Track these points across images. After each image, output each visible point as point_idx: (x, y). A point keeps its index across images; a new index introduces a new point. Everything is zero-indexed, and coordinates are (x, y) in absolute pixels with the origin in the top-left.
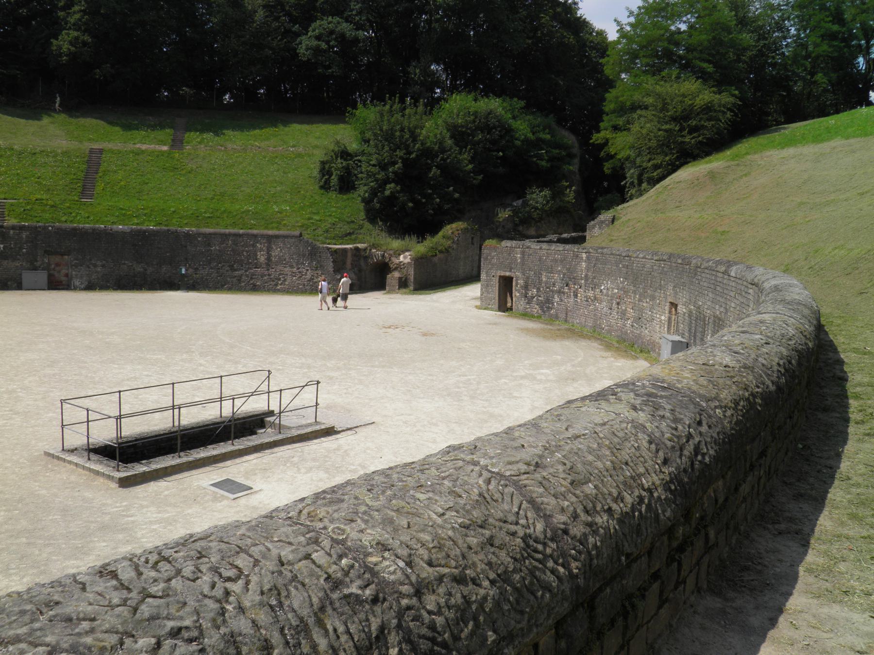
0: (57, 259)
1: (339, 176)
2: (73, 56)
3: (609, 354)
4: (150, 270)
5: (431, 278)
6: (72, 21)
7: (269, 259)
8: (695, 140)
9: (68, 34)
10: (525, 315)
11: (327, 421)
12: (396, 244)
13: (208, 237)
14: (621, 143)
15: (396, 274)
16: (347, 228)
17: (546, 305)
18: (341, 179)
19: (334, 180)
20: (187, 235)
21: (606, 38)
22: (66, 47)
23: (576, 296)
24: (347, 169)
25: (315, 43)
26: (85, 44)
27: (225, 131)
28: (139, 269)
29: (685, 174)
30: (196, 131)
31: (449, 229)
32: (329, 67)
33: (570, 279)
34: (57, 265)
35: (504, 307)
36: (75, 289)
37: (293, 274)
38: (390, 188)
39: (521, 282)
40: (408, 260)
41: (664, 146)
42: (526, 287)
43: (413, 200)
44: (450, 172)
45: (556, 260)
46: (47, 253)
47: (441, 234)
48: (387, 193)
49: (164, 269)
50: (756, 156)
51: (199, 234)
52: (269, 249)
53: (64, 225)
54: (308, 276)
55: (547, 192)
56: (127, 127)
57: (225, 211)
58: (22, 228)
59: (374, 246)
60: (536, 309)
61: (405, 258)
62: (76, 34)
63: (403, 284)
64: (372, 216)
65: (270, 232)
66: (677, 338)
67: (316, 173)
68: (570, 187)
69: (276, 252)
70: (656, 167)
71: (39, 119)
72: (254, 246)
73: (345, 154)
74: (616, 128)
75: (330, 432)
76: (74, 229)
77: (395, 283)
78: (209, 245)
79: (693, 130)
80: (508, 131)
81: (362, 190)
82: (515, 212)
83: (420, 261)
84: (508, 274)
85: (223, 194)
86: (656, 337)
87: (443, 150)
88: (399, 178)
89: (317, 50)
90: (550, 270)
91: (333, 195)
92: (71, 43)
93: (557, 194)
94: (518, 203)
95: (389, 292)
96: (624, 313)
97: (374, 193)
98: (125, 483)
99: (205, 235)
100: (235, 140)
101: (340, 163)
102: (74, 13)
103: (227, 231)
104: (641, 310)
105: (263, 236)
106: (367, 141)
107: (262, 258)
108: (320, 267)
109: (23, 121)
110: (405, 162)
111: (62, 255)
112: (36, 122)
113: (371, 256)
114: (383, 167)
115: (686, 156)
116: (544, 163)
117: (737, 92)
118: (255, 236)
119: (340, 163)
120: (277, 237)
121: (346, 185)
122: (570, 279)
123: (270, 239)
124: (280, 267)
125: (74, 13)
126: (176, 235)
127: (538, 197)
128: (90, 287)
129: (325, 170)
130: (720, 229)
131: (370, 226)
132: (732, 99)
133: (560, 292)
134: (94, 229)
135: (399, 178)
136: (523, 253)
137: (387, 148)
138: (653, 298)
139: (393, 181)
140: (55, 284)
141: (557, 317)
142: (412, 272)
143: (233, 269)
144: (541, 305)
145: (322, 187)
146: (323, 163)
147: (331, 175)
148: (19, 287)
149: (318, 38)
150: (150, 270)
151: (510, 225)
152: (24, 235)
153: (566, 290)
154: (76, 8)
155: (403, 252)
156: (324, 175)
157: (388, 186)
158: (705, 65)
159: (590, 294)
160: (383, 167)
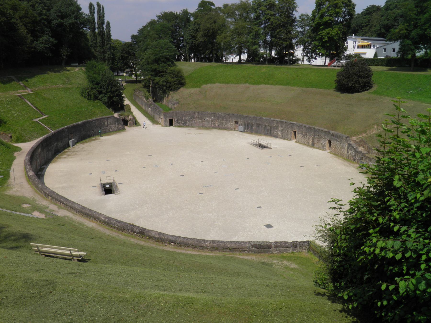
23: (195, 121)
33: (193, 118)
42: (178, 120)
52: (107, 121)
60: (181, 125)
105: (106, 118)
107: (106, 124)
120: (109, 117)
121: (96, 98)
123: (108, 118)
133: (189, 121)
136: (176, 113)
139: (115, 97)
144: (183, 124)
145: (88, 99)
156: (89, 95)
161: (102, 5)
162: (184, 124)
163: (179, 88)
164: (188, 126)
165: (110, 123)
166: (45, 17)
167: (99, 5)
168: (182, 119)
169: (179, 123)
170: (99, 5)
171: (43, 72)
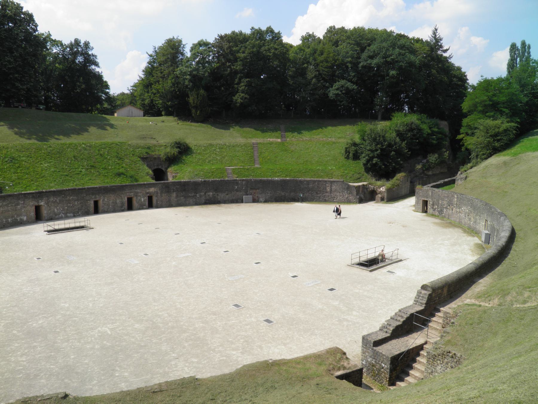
0: (254, 191)
1: (353, 153)
2: (241, 104)
3: (465, 235)
4: (287, 194)
5: (393, 197)
6: (241, 89)
7: (331, 190)
8: (500, 144)
9: (240, 95)
10: (433, 215)
11: (400, 258)
12: (379, 183)
13: (308, 182)
14: (470, 142)
15: (380, 196)
16: (358, 176)
17: (441, 212)
18: (354, 154)
19: (351, 155)
20: (301, 181)
21: (462, 78)
22: (239, 100)
23: (452, 210)
24: (356, 151)
25: (337, 92)
26: (246, 98)
27: (302, 132)
28: (283, 194)
29: (495, 160)
30: (290, 132)
31: (400, 176)
32: (342, 101)
33: (450, 204)
34: (254, 193)
35: (425, 211)
36: (261, 202)
37: (340, 196)
38: (375, 160)
39: (431, 203)
40: (384, 190)
41: (487, 146)
42: (433, 205)
43: (384, 164)
44: (399, 152)
45: (445, 196)
46: (251, 189)
47: (395, 178)
48: (374, 162)
49: (292, 194)
50: (523, 155)
51: (305, 181)
52: (331, 186)
53: (257, 179)
54: (346, 197)
55: (436, 155)
56: (263, 131)
57: (310, 170)
58: (243, 180)
59: (370, 184)
60: (437, 213)
61: (383, 189)
62: (243, 95)
63: (382, 199)
64: (367, 170)
65: (332, 180)
66: (487, 232)
67: (343, 151)
68: (446, 152)
69: (334, 187)
70: (484, 154)
71: (229, 130)
72: (325, 185)
73: (355, 144)
74: (467, 134)
75: (401, 261)
76: (261, 180)
77: (380, 199)
78: (309, 185)
79: (498, 141)
80: (420, 130)
81: (363, 160)
82: (424, 166)
83: (389, 190)
84: (426, 199)
85: (307, 161)
86: (481, 229)
87: (395, 144)
88: (378, 156)
89: (337, 95)
90: (443, 200)
91: (351, 161)
92: (241, 99)
93: (441, 155)
94: (425, 161)
95: (377, 202)
96: (470, 219)
97: (368, 161)
98: (371, 271)
99: (307, 181)
100: (306, 136)
101: (353, 148)
102: (242, 86)
103: (315, 179)
104: (476, 219)
105: (329, 181)
106: (364, 140)
107: (328, 189)
108: (351, 193)
109: (223, 131)
110: (382, 150)
111: (256, 189)
112: (228, 131)
113: (369, 188)
114: (372, 151)
115: (495, 151)
116: (435, 142)
117: (519, 120)
118: (326, 181)
119: (353, 148)
120: (334, 182)
121: (356, 157)
122: (450, 204)
123: (332, 182)
124: (335, 193)
125: (242, 86)
126: (296, 181)
127: (433, 158)
128: (266, 201)
129: (347, 151)
130: (505, 190)
131: (367, 175)
132: (516, 125)
133: (446, 208)
134: (267, 180)
135: (378, 156)
136: (432, 192)
137: (374, 144)
138: (480, 216)
139: (376, 157)
140: (255, 201)
141: (445, 217)
142: (386, 194)
143: (317, 193)
144: (439, 212)
145: (345, 158)
146: (346, 148)
147: (350, 153)
148: (242, 202)
149: (337, 89)
150: (287, 194)
151: (421, 171)
152: (244, 183)
153: (449, 207)
154: (242, 84)
155: (382, 186)
156: (346, 153)
157: (375, 159)
158: (504, 110)
159: (458, 210)
160: (372, 151)
161: (527, 44)
162: (440, 214)
163: (490, 155)
164: (443, 218)
165: (336, 190)
166: (350, 59)
167: (523, 44)
168: (439, 203)
169: (434, 210)
170: (523, 44)
171: (344, 124)
